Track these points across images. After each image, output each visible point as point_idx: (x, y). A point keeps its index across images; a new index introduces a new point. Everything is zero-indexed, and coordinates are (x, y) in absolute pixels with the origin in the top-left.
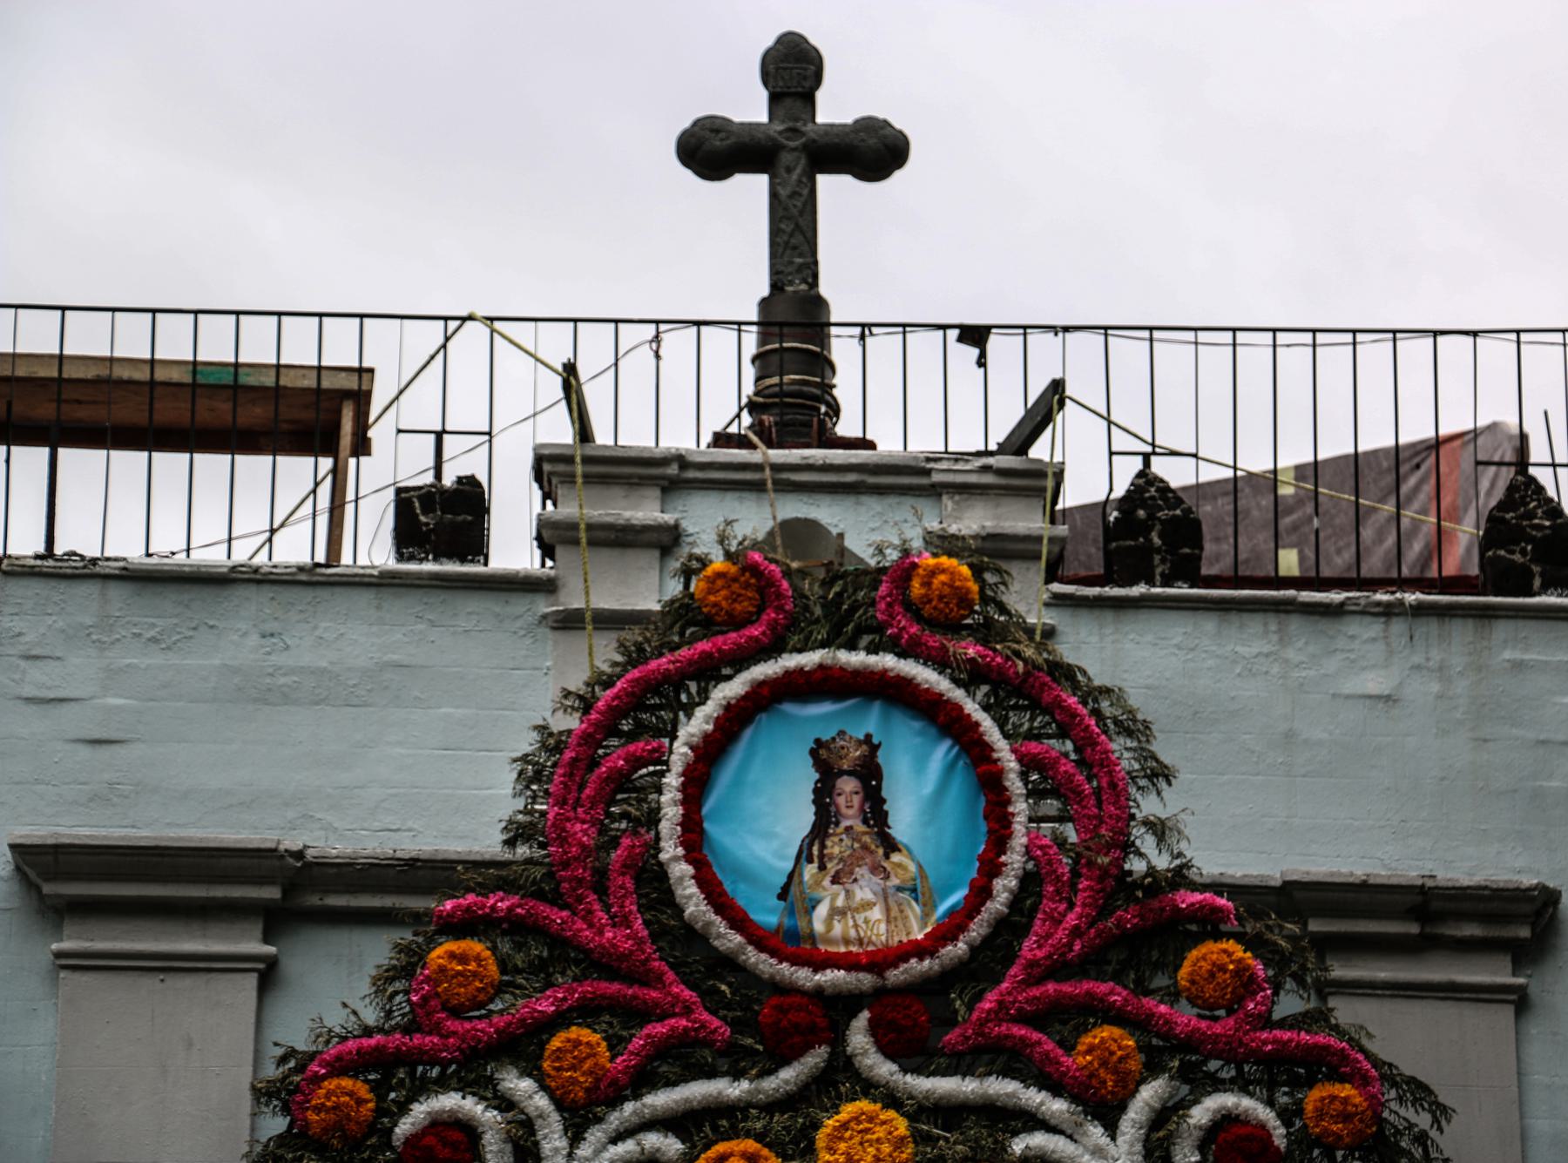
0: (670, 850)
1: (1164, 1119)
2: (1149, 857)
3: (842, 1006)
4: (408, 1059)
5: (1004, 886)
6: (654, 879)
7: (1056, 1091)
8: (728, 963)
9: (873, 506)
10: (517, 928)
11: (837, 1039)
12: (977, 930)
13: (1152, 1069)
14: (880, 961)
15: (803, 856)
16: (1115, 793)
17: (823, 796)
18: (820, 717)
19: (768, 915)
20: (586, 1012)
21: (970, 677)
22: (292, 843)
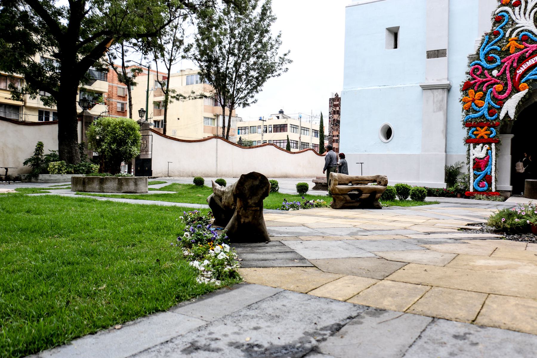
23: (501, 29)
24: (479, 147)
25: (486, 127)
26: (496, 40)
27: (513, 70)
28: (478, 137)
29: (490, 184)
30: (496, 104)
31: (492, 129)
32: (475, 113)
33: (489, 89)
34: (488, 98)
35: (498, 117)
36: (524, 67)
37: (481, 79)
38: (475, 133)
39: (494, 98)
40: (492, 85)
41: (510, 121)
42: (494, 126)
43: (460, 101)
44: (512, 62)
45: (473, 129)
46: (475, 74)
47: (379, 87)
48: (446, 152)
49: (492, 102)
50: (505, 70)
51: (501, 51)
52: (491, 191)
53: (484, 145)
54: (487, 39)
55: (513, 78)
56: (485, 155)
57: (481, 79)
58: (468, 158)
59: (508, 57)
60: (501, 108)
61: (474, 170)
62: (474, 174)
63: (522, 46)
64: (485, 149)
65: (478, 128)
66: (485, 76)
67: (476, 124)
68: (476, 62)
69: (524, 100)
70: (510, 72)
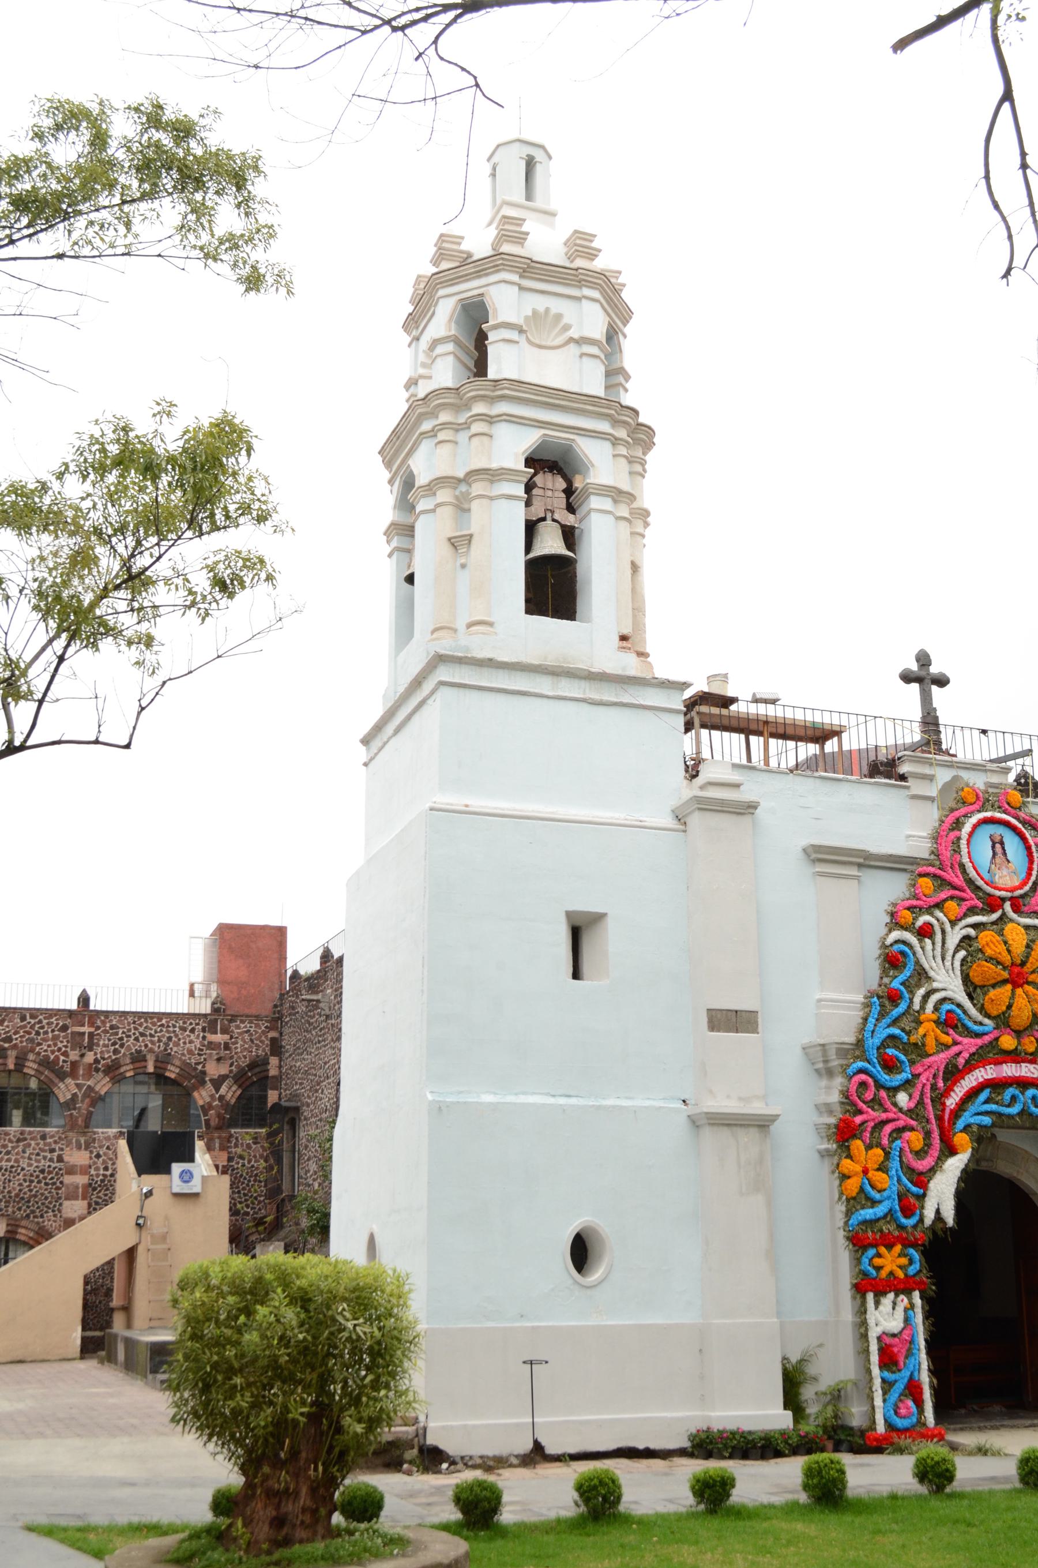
0: (965, 860)
3: (1003, 900)
4: (915, 907)
6: (962, 866)
8: (978, 888)
9: (972, 773)
10: (935, 876)
11: (1001, 906)
12: (1030, 884)
14: (1012, 890)
15: (991, 863)
17: (993, 847)
19: (986, 876)
20: (952, 898)
21: (1024, 823)
22: (868, 849)
23: (902, 988)
25: (898, 1248)
27: (939, 1100)
28: (884, 1274)
29: (919, 1403)
30: (911, 1182)
31: (912, 1251)
32: (872, 1207)
33: (893, 1141)
34: (895, 1164)
35: (921, 1220)
38: (878, 1261)
39: (909, 1170)
40: (900, 1131)
41: (946, 1230)
42: (914, 1245)
43: (833, 1172)
44: (934, 1075)
45: (871, 1252)
46: (859, 1098)
47: (551, 1100)
48: (779, 1314)
49: (905, 1180)
50: (922, 1094)
52: (924, 1424)
53: (897, 1296)
54: (876, 1010)
55: (940, 1119)
56: (902, 1325)
58: (865, 1337)
59: (927, 1061)
60: (924, 1195)
61: (881, 1368)
62: (884, 1380)
63: (947, 1039)
65: (883, 1250)
66: (881, 1105)
67: (878, 1237)
68: (860, 1064)
70: (932, 1101)
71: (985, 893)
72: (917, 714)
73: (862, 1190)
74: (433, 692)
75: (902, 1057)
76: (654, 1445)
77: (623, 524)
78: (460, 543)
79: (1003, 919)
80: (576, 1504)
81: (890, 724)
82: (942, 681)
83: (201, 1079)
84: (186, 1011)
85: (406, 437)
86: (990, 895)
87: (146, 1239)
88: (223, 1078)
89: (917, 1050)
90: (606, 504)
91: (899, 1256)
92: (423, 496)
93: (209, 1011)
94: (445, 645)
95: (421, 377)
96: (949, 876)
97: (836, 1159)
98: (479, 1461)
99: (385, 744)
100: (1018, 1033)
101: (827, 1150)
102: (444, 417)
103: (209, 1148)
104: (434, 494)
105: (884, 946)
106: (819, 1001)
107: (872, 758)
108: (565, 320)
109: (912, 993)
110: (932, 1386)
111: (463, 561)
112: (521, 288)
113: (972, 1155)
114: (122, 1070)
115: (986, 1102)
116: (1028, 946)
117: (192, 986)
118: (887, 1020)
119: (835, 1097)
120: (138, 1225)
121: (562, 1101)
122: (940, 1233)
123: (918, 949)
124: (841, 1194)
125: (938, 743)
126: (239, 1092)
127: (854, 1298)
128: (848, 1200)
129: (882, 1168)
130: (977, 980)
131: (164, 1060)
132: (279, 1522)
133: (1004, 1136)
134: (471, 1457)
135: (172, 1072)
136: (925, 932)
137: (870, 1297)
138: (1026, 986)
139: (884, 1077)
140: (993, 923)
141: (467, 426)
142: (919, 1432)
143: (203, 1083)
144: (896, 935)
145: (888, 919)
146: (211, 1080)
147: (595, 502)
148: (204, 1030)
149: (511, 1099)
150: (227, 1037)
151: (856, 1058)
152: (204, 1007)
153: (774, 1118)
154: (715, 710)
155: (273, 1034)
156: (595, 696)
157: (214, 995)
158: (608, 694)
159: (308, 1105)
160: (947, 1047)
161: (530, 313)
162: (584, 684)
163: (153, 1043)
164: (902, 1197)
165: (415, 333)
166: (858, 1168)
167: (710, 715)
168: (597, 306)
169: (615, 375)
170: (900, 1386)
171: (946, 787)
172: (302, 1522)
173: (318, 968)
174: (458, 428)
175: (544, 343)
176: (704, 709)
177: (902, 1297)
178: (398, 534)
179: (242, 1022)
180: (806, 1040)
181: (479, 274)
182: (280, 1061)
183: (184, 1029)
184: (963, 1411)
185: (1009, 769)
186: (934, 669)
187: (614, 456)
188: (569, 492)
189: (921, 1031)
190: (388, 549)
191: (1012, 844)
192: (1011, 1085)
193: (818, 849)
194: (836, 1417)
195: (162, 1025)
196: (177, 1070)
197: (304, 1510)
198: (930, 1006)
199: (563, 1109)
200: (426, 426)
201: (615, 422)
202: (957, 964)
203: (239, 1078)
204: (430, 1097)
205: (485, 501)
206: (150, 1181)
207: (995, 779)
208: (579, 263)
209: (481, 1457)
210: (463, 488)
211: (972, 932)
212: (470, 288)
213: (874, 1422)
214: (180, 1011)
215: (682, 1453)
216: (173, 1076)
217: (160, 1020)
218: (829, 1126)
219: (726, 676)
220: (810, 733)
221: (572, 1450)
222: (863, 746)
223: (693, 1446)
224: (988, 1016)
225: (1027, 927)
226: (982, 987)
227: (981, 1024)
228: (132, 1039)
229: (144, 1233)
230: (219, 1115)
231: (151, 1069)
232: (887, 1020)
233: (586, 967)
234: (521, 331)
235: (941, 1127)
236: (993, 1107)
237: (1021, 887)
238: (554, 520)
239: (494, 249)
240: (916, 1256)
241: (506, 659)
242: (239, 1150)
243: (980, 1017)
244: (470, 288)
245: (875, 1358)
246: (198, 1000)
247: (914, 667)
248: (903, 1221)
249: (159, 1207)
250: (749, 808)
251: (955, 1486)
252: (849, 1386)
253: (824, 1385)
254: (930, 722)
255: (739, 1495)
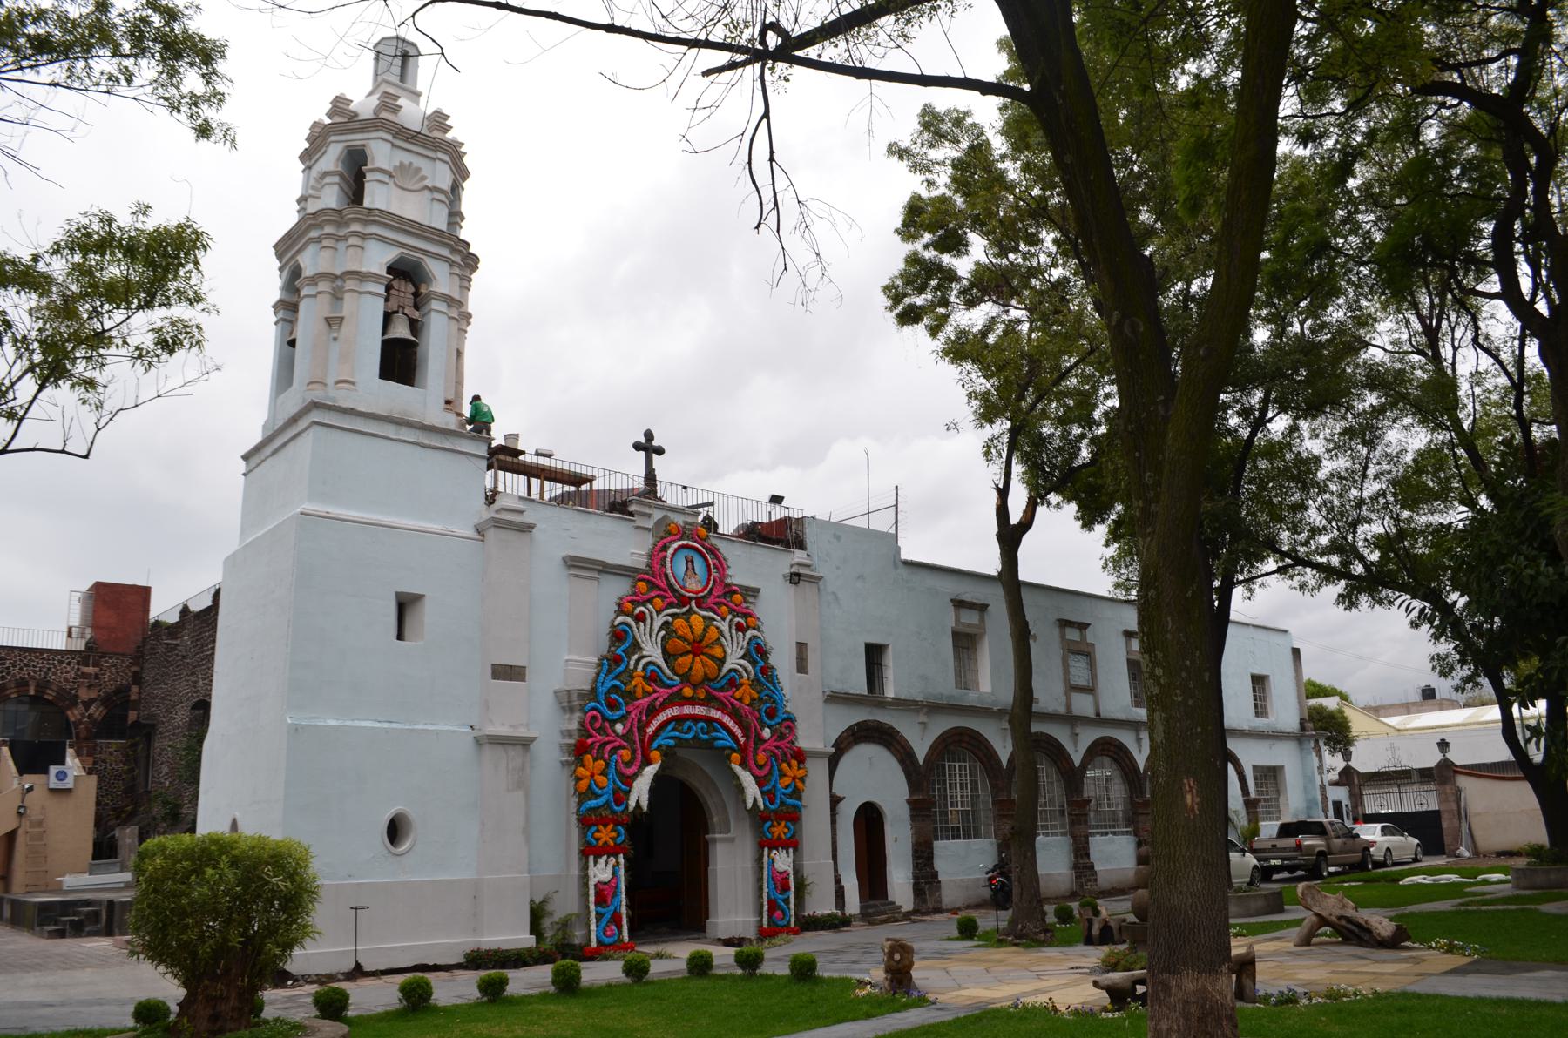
0: (669, 571)
1: (731, 621)
2: (728, 581)
3: (690, 599)
5: (711, 582)
6: (666, 575)
7: (718, 615)
8: (676, 590)
10: (647, 581)
13: (730, 613)
14: (697, 593)
16: (723, 568)
18: (686, 552)
20: (658, 596)
24: (602, 860)
26: (619, 670)
28: (601, 843)
29: (620, 927)
31: (620, 828)
34: (612, 771)
35: (627, 807)
36: (655, 723)
37: (601, 738)
38: (597, 835)
39: (621, 775)
40: (616, 749)
42: (621, 824)
44: (641, 713)
45: (594, 829)
47: (378, 725)
48: (529, 871)
49: (617, 780)
50: (632, 724)
51: (625, 691)
53: (608, 857)
54: (606, 667)
55: (642, 741)
57: (601, 738)
58: (586, 885)
59: (636, 703)
60: (630, 791)
62: (597, 913)
63: (651, 689)
64: (610, 868)
65: (601, 827)
66: (605, 731)
68: (593, 704)
69: (657, 779)
71: (680, 594)
72: (642, 472)
73: (589, 787)
74: (306, 429)
75: (621, 700)
76: (440, 962)
77: (453, 323)
78: (333, 322)
79: (690, 611)
80: (400, 1000)
81: (625, 477)
82: (660, 451)
83: (73, 701)
84: (64, 648)
85: (298, 237)
86: (683, 596)
87: (25, 824)
88: (92, 701)
89: (630, 696)
90: (443, 307)
91: (612, 831)
92: (308, 285)
93: (83, 649)
94: (317, 395)
95: (311, 196)
96: (658, 581)
97: (573, 768)
98: (315, 978)
99: (263, 461)
100: (695, 687)
101: (567, 761)
102: (328, 229)
103: (78, 754)
104: (316, 284)
105: (613, 626)
106: (567, 661)
107: (612, 499)
108: (423, 173)
109: (629, 658)
110: (628, 916)
111: (335, 335)
112: (393, 145)
113: (661, 765)
114: (8, 692)
115: (673, 730)
116: (704, 630)
117: (70, 629)
118: (613, 675)
119: (574, 726)
120: (19, 813)
121: (386, 725)
122: (639, 817)
123: (635, 629)
124: (576, 790)
125: (655, 492)
126: (105, 712)
127: (580, 859)
128: (580, 794)
129: (604, 773)
130: (671, 651)
131: (43, 685)
132: (214, 1018)
133: (681, 753)
134: (309, 976)
135: (50, 695)
136: (640, 618)
137: (591, 858)
138: (703, 657)
139: (609, 713)
140: (684, 614)
141: (345, 238)
142: (618, 946)
143: (75, 704)
144: (621, 619)
145: (616, 608)
146: (83, 703)
147: (435, 305)
148: (78, 663)
149: (348, 723)
150: (97, 669)
151: (591, 700)
152: (80, 645)
153: (533, 739)
154: (509, 459)
155: (134, 668)
156: (426, 442)
157: (88, 637)
158: (435, 441)
159: (163, 723)
160: (649, 694)
161: (398, 164)
162: (418, 432)
163: (34, 672)
164: (616, 792)
165: (307, 163)
166: (588, 773)
167: (506, 461)
168: (447, 167)
169: (455, 216)
170: (608, 916)
171: (659, 522)
172: (232, 1017)
173: (177, 619)
174: (338, 239)
175: (405, 187)
176: (502, 457)
177: (612, 858)
178: (284, 309)
179: (111, 658)
180: (557, 687)
181: (363, 130)
182: (140, 688)
183: (61, 662)
184: (643, 932)
185: (699, 513)
186: (655, 443)
187: (451, 274)
188: (416, 294)
189: (633, 683)
190: (275, 319)
191: (699, 564)
192: (688, 720)
193: (573, 558)
194: (564, 938)
195: (44, 659)
196: (54, 694)
197: (233, 1009)
198: (640, 667)
199: (386, 731)
200: (314, 234)
201: (454, 250)
202: (659, 640)
203: (106, 701)
204: (289, 721)
205: (355, 294)
206: (29, 780)
207: (690, 519)
208: (436, 134)
209: (317, 975)
210: (339, 283)
211: (670, 619)
212: (356, 139)
213: (589, 940)
214: (59, 648)
215: (459, 966)
216: (50, 698)
217: (42, 654)
218: (570, 745)
219: (517, 435)
220: (572, 479)
221: (382, 968)
222: (607, 488)
223: (467, 962)
224: (677, 675)
225: (704, 617)
226: (674, 655)
227: (672, 679)
228: (17, 669)
229: (23, 820)
230: (87, 728)
231: (32, 692)
232: (613, 675)
233: (407, 632)
234: (391, 176)
235: (643, 747)
236: (677, 734)
237: (702, 591)
238: (404, 314)
239: (375, 114)
240: (622, 831)
241: (363, 410)
242: (102, 756)
243: (672, 675)
244: (356, 139)
245: (592, 898)
246: (74, 640)
247: (643, 440)
248: (616, 808)
249: (37, 800)
250: (528, 528)
251: (649, 977)
252: (574, 918)
253: (556, 918)
254: (650, 477)
255: (513, 989)
